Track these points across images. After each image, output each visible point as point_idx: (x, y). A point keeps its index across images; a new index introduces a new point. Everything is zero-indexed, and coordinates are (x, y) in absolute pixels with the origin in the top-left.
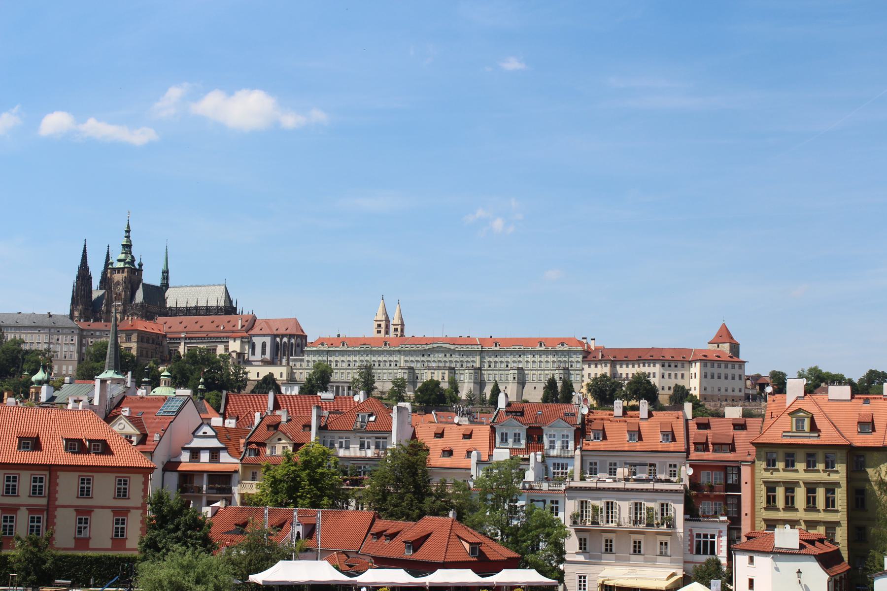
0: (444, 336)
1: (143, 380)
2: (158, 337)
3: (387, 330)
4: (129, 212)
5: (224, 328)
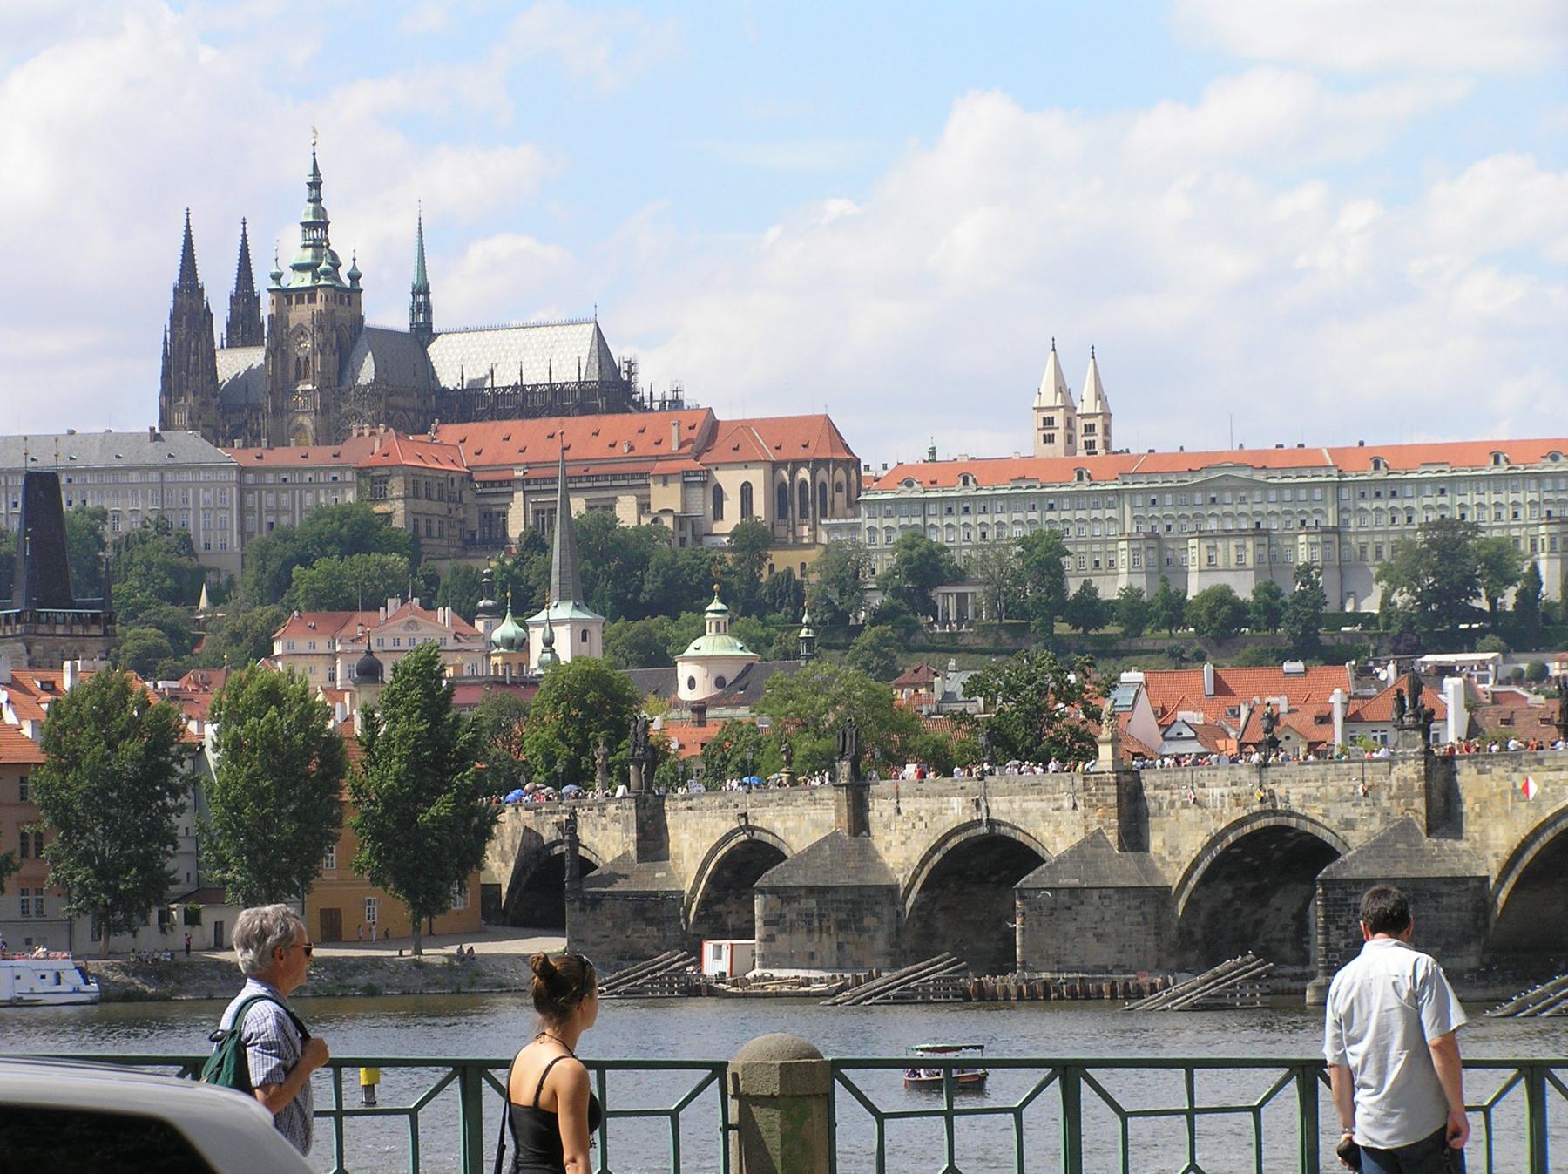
0: (1236, 447)
1: (481, 603)
2: (452, 479)
3: (1070, 432)
4: (315, 131)
5: (631, 449)
